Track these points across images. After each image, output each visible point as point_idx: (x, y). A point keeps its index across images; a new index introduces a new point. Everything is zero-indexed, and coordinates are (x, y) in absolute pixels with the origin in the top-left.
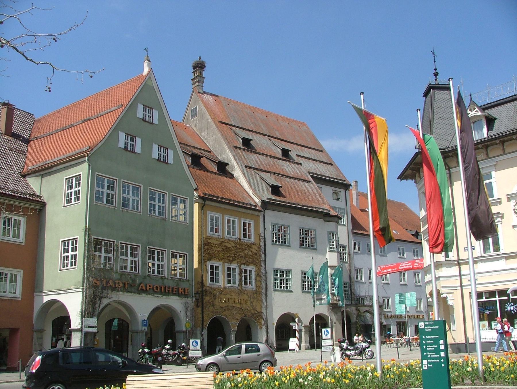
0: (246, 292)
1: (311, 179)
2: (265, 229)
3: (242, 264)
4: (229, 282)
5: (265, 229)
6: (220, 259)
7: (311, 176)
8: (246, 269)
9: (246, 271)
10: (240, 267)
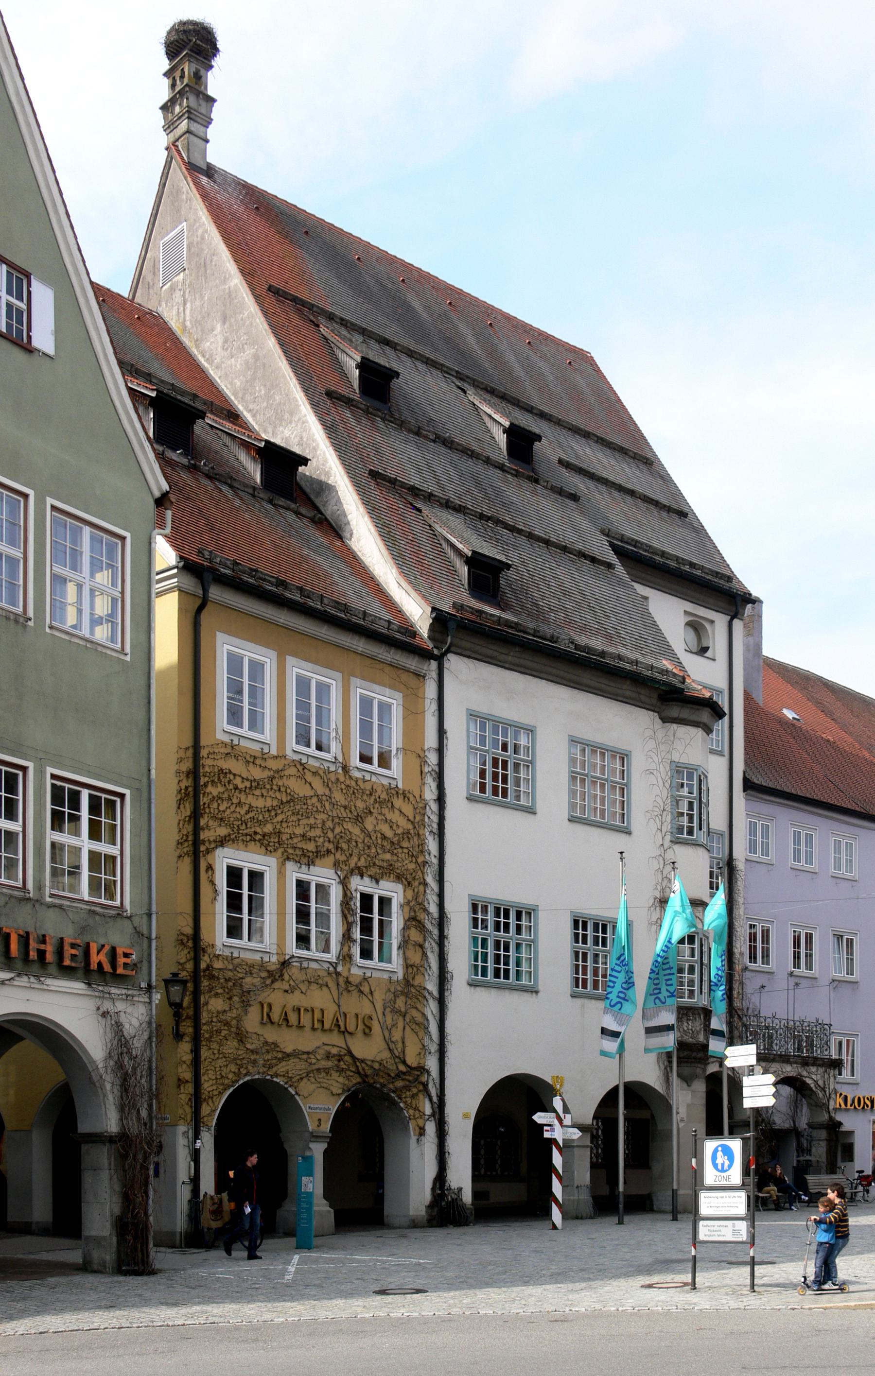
0: (366, 989)
1: (613, 558)
2: (442, 732)
3: (352, 872)
4: (303, 940)
5: (442, 732)
6: (267, 843)
7: (612, 545)
8: (368, 890)
10: (344, 883)
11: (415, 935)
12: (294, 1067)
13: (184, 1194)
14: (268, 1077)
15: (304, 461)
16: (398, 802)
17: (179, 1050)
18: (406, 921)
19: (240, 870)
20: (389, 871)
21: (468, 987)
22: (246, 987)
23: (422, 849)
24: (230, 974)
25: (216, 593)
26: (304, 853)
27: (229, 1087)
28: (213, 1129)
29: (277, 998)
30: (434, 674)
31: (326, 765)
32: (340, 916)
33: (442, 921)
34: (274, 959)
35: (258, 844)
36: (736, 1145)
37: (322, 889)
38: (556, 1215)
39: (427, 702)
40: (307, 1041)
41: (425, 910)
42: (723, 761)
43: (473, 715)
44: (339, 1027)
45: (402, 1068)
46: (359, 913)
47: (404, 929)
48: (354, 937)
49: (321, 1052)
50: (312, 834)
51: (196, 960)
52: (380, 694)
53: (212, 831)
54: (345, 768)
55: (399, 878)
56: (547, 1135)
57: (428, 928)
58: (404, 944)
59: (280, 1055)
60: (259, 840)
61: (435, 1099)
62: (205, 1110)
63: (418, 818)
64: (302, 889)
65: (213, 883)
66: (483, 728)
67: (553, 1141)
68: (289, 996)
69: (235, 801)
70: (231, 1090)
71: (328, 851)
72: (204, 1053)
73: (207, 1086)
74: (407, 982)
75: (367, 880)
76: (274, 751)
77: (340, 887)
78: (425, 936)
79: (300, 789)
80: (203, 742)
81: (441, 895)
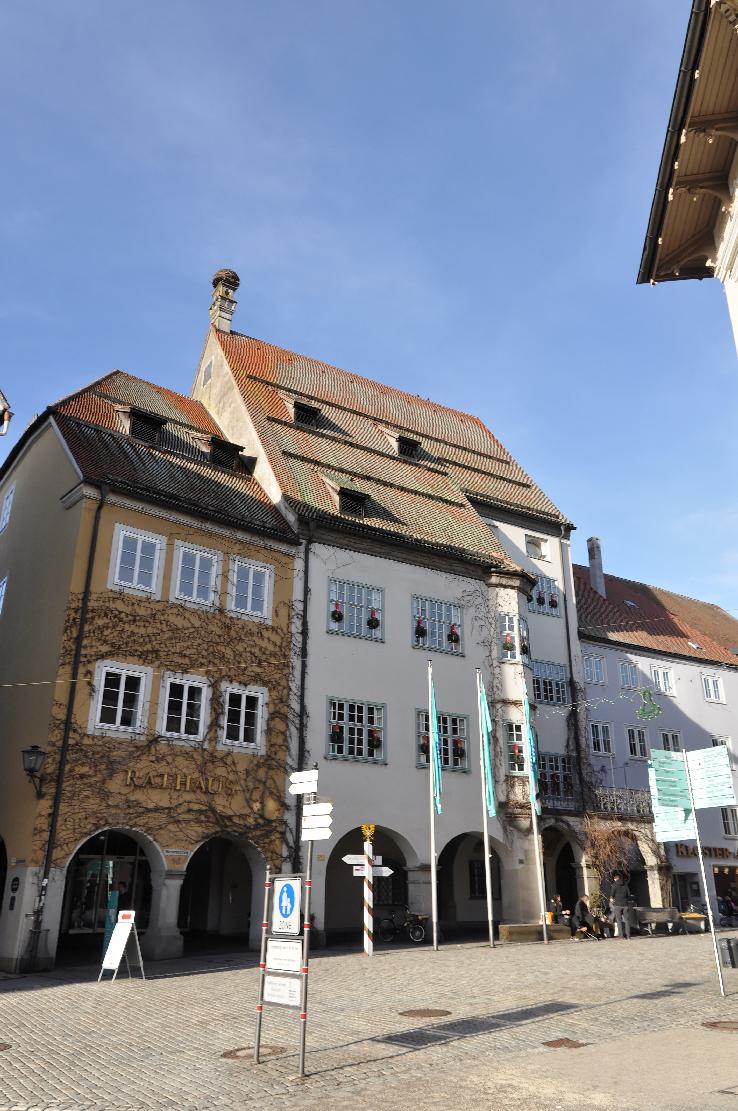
0: (229, 761)
2: (307, 590)
3: (222, 678)
4: (173, 724)
5: (307, 590)
6: (144, 658)
7: (467, 497)
8: (235, 691)
9: (235, 699)
10: (214, 686)
11: (279, 725)
12: (153, 820)
13: (23, 926)
14: (127, 827)
15: (242, 449)
16: (266, 634)
17: (40, 807)
18: (271, 714)
19: (181, 687)
20: (257, 679)
22: (112, 759)
24: (99, 749)
25: (112, 498)
26: (179, 666)
27: (87, 834)
28: (65, 869)
29: (143, 767)
30: (302, 555)
31: (204, 608)
33: (303, 713)
34: (143, 738)
36: (296, 884)
37: (194, 692)
38: (368, 943)
39: (296, 572)
41: (289, 706)
42: (562, 621)
43: (333, 580)
45: (261, 821)
46: (227, 707)
47: (269, 720)
50: (187, 652)
51: (66, 738)
52: (254, 566)
53: (91, 645)
54: (221, 611)
55: (265, 684)
56: (356, 874)
57: (289, 717)
58: (269, 731)
59: (141, 810)
60: (138, 655)
61: (292, 843)
62: (57, 853)
63: (284, 644)
64: (176, 690)
65: (90, 684)
66: (341, 588)
68: (156, 765)
69: (118, 629)
70: (88, 838)
71: (202, 664)
72: (63, 808)
73: (63, 834)
74: (268, 757)
75: (235, 684)
76: (158, 597)
77: (210, 691)
78: (287, 725)
79: (179, 622)
80: (93, 588)
81: (302, 697)
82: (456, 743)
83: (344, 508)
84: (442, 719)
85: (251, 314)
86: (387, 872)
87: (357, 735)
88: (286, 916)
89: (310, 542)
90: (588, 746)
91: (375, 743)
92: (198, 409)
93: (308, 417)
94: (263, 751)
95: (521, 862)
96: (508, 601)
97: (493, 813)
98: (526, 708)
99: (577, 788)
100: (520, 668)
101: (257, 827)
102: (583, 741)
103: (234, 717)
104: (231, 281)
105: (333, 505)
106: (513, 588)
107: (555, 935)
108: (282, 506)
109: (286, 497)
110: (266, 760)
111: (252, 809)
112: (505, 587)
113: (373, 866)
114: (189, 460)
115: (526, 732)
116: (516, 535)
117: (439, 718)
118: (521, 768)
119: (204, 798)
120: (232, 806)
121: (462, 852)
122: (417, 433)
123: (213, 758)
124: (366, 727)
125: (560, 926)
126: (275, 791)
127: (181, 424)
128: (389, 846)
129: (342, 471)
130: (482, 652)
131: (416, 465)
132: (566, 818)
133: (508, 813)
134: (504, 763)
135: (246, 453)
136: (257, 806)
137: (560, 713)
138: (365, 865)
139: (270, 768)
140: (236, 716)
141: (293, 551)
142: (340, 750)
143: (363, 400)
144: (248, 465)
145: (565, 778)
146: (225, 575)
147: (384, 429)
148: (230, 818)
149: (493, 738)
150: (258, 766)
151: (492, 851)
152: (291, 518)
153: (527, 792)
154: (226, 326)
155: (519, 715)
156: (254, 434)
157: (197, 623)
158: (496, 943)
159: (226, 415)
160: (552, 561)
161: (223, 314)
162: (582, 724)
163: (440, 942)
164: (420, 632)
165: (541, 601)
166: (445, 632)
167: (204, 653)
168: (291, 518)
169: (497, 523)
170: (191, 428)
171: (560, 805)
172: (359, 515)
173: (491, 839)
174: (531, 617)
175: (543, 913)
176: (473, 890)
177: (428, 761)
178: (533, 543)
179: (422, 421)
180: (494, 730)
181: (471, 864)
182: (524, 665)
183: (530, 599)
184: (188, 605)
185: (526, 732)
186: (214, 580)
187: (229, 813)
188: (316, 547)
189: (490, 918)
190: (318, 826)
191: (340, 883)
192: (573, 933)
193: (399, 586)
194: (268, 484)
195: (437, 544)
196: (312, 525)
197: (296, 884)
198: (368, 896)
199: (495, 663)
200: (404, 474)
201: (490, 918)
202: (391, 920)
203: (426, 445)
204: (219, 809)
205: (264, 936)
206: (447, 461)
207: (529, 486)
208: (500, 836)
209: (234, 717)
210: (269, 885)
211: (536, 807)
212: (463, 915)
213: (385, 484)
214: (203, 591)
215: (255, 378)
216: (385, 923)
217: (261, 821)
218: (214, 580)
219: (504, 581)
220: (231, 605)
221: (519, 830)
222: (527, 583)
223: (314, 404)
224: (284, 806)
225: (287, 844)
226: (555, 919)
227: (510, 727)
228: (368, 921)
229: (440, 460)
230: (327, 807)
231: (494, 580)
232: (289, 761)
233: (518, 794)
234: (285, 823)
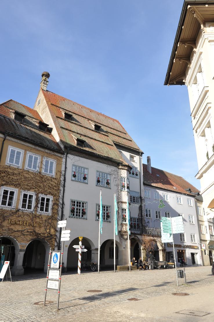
0: (40, 217)
2: (66, 168)
3: (39, 193)
4: (24, 206)
5: (66, 168)
6: (16, 186)
8: (44, 197)
9: (43, 199)
10: (37, 195)
11: (56, 207)
15: (48, 125)
20: (50, 193)
21: (69, 218)
23: (59, 189)
25: (8, 138)
26: (27, 189)
29: (14, 218)
30: (65, 157)
31: (35, 172)
32: (35, 201)
35: (13, 186)
36: (59, 254)
38: (79, 271)
40: (19, 228)
41: (59, 201)
42: (139, 180)
44: (31, 225)
45: (49, 235)
46: (40, 201)
48: (38, 206)
49: (26, 231)
50: (29, 185)
52: (50, 160)
54: (40, 173)
55: (52, 195)
56: (76, 251)
57: (59, 204)
58: (53, 209)
61: (58, 242)
64: (25, 196)
66: (76, 168)
67: (78, 252)
69: (8, 177)
71: (33, 188)
74: (52, 216)
75: (43, 195)
76: (21, 168)
77: (36, 196)
79: (27, 176)
82: (107, 214)
83: (78, 144)
84: (104, 207)
85: (53, 85)
86: (86, 250)
87: (78, 210)
88: (55, 263)
89: (67, 154)
90: (144, 215)
91: (84, 213)
92: (36, 113)
93: (68, 117)
94: (50, 215)
95: (124, 248)
96: (124, 173)
97: (117, 234)
98: (127, 204)
99: (141, 227)
100: (127, 193)
101: (48, 237)
102: (143, 214)
103: (42, 204)
104: (48, 75)
105: (75, 143)
106: (124, 169)
107: (133, 269)
108: (60, 143)
109: (61, 140)
110: (51, 217)
111: (46, 231)
112: (123, 169)
113: (82, 248)
114: (32, 128)
115: (127, 211)
116: (127, 154)
117: (103, 206)
118: (125, 221)
119: (32, 228)
120: (41, 230)
121: (107, 245)
122: (100, 124)
123: (36, 216)
124: (81, 208)
125: (134, 266)
126: (54, 226)
127: (30, 117)
128: (86, 243)
129: (78, 133)
130: (116, 188)
131: (99, 133)
132: (137, 236)
133: (121, 234)
134: (121, 219)
135: (49, 127)
136: (48, 231)
137: (137, 206)
138: (79, 248)
139: (53, 219)
140: (43, 204)
141: (62, 156)
142: (74, 215)
143: (84, 113)
144: (50, 130)
145: (138, 224)
146: (42, 162)
147: (91, 122)
148: (40, 234)
149: (118, 212)
150: (49, 219)
151: (116, 245)
152: (62, 146)
153: (127, 228)
154: (45, 89)
155: (126, 206)
156: (52, 121)
157: (32, 176)
158: (116, 271)
159: (44, 115)
160: (137, 163)
161: (44, 85)
162: (143, 210)
163: (100, 271)
164: (98, 181)
165: (133, 174)
166: (106, 182)
167: (34, 185)
168: (62, 146)
169: (122, 151)
170: (33, 118)
171: (136, 232)
172: (82, 147)
173: (116, 241)
174: (130, 178)
175: (129, 263)
176: (110, 256)
177: (99, 218)
178: (132, 157)
179: (102, 120)
180: (118, 210)
181: (110, 248)
182: (128, 192)
183: (130, 173)
184: (30, 171)
185: (127, 211)
186: (38, 164)
187: (40, 232)
188: (69, 155)
189: (115, 264)
190: (66, 237)
191: (72, 253)
192: (138, 268)
193: (93, 168)
194: (56, 136)
195: (105, 156)
196: (68, 149)
197: (59, 254)
198: (80, 257)
199: (119, 191)
200: (96, 135)
201: (115, 264)
202: (86, 264)
203: (103, 127)
204: (37, 231)
205: (48, 269)
206: (108, 132)
207: (131, 141)
208: (118, 241)
209: (42, 204)
210: (51, 254)
211: (129, 232)
212: (107, 263)
213: (90, 138)
214: (35, 167)
215: (53, 105)
216: (84, 265)
217: (49, 235)
218: (38, 164)
219: (123, 168)
220: (43, 171)
221: (124, 239)
222: (130, 168)
223: (70, 113)
224: (56, 231)
225: (57, 242)
226: (133, 264)
227: (123, 210)
228: (79, 264)
229: (106, 132)
230: (69, 231)
231: (120, 167)
232: (58, 217)
233: (124, 229)
234: (56, 236)
